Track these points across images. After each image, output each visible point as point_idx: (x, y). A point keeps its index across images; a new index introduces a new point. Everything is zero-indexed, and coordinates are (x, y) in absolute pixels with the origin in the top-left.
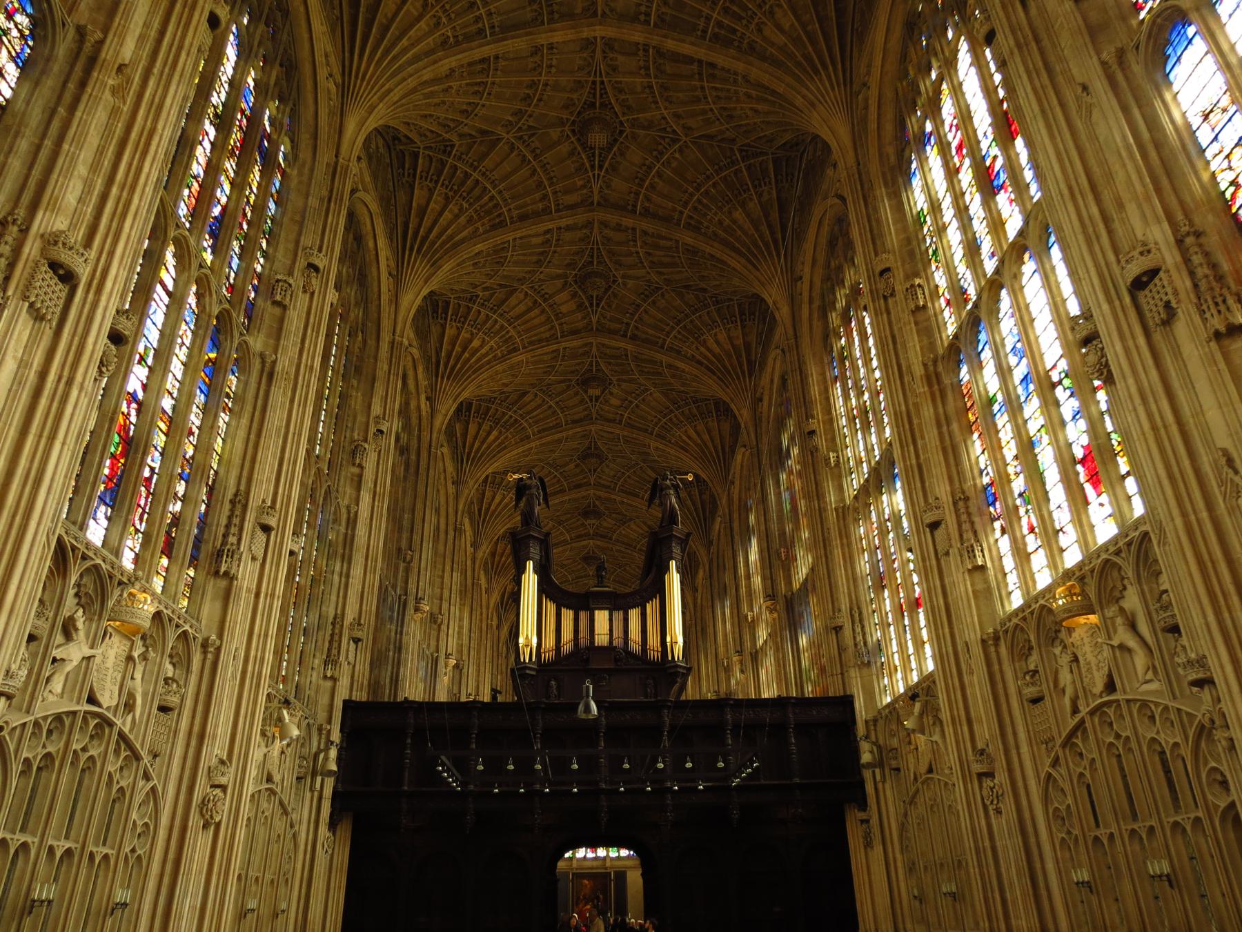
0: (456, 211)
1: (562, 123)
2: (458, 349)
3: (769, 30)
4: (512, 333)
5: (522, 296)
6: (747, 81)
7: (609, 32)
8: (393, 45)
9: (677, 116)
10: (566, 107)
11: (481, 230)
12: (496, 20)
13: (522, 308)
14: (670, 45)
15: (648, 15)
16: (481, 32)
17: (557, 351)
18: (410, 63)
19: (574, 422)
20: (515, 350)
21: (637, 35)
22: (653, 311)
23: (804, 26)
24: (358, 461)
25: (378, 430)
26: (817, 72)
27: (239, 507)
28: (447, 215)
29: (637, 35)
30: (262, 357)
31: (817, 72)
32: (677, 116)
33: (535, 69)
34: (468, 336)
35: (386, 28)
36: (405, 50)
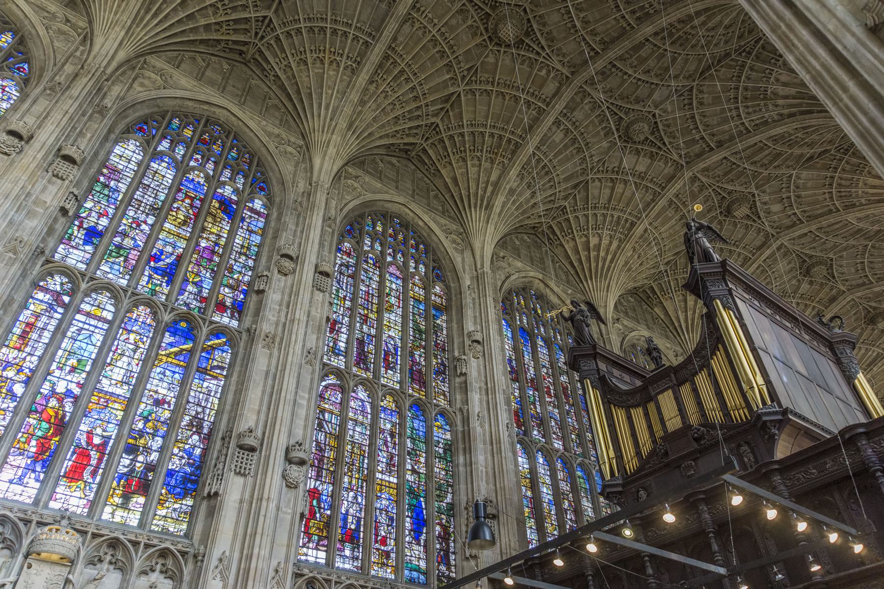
0: (477, 163)
2: (583, 254)
4: (616, 214)
5: (597, 183)
11: (506, 162)
13: (607, 191)
17: (671, 202)
19: (760, 248)
20: (633, 224)
22: (708, 110)
24: (459, 372)
25: (474, 341)
27: (227, 439)
28: (473, 171)
30: (248, 330)
34: (584, 239)
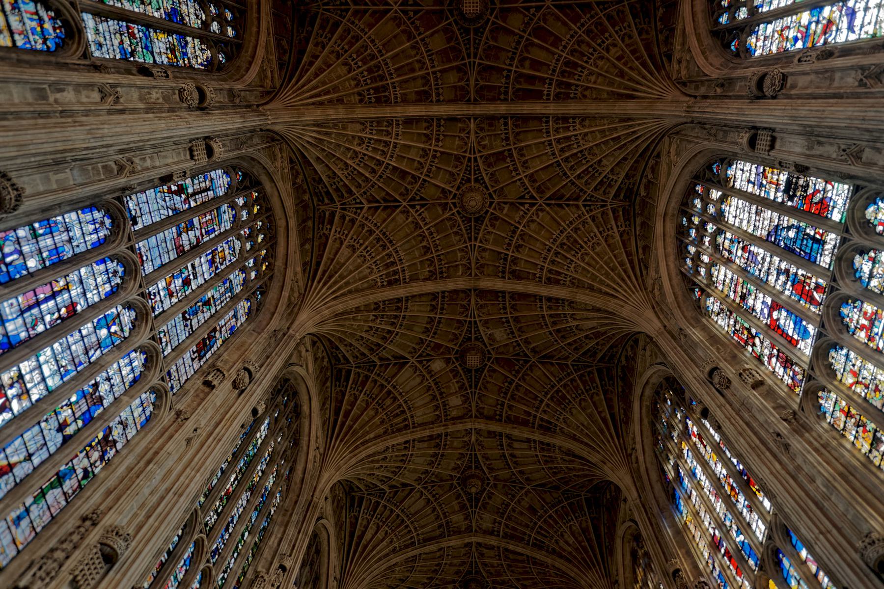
1: (454, 581)
3: (562, 543)
6: (554, 566)
7: (480, 540)
8: (368, 555)
9: (518, 580)
10: (457, 573)
12: (421, 537)
14: (511, 547)
15: (499, 532)
16: (413, 544)
18: (376, 562)
21: (493, 541)
23: (579, 543)
26: (590, 569)
29: (493, 541)
31: (590, 569)
32: (518, 580)
33: (439, 557)
35: (366, 547)
36: (374, 556)
